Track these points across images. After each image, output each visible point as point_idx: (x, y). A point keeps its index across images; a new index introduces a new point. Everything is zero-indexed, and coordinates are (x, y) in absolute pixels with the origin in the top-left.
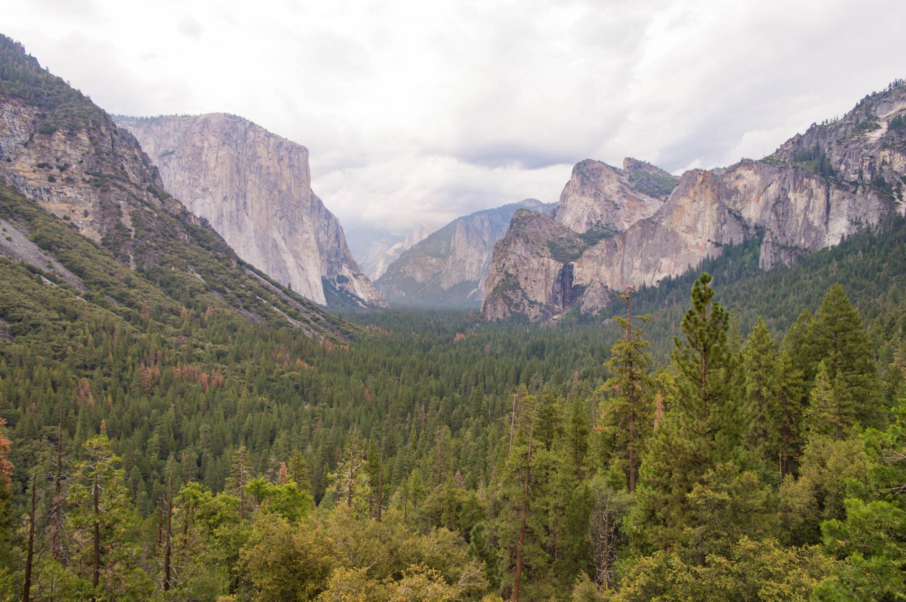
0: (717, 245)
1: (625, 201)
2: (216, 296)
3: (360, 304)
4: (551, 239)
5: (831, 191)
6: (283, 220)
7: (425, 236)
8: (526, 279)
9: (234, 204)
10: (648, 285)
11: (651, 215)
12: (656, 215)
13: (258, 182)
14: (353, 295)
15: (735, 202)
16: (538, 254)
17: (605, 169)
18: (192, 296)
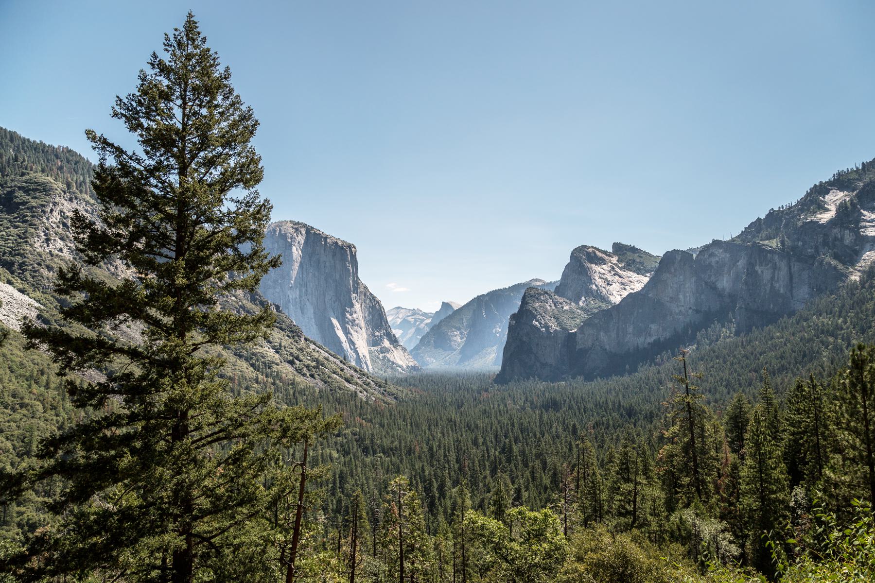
0: (697, 311)
1: (617, 277)
2: (287, 365)
3: (400, 369)
4: (556, 312)
5: (792, 264)
6: (337, 303)
7: (450, 313)
8: (537, 345)
9: (298, 293)
10: (641, 346)
11: (639, 289)
12: (643, 289)
13: (317, 274)
14: (393, 363)
15: (710, 276)
16: (546, 323)
17: (597, 252)
18: (270, 368)
